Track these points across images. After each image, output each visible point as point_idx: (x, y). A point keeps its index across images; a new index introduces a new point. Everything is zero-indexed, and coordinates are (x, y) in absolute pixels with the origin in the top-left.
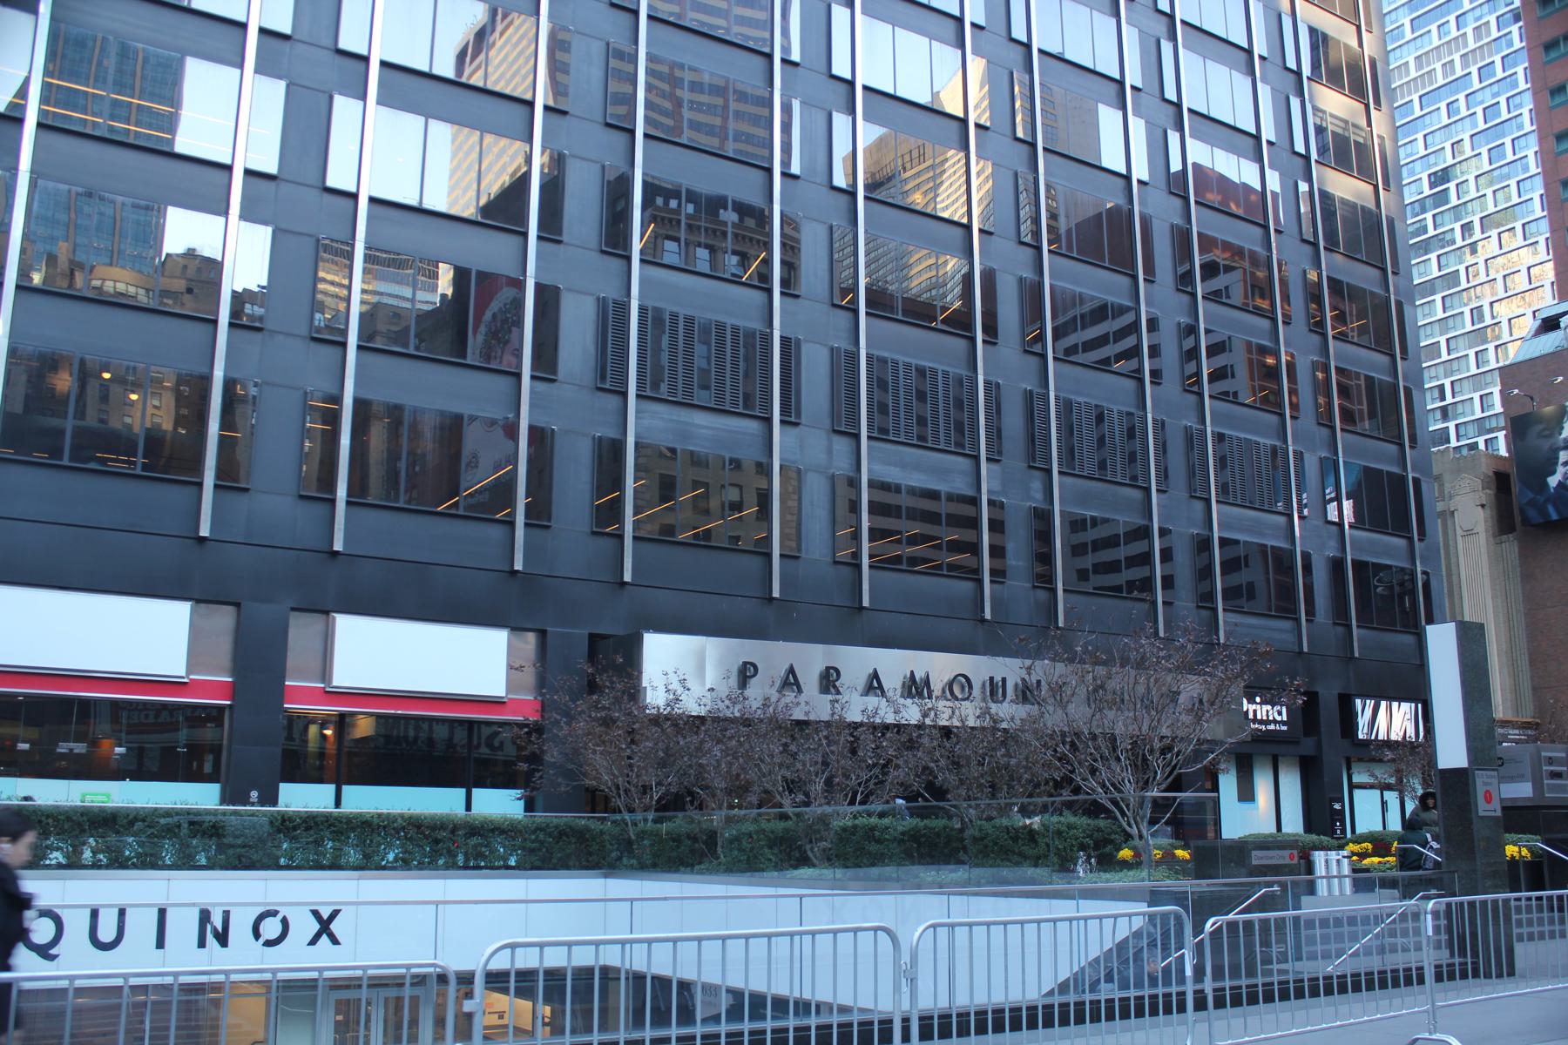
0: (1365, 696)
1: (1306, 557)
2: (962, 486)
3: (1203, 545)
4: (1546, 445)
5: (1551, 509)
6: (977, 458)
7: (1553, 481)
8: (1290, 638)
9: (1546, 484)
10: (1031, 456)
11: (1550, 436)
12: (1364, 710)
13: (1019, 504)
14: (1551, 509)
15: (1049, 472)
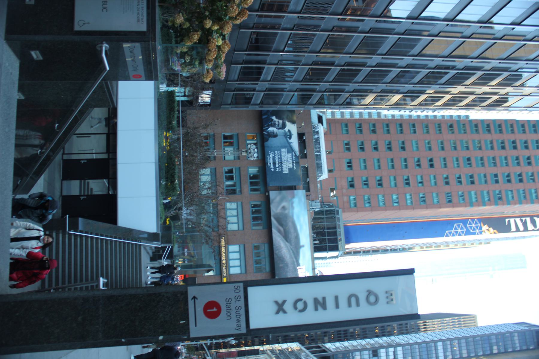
0: (213, 93)
1: (257, 84)
2: (291, 7)
3: (264, 63)
4: (285, 117)
5: (266, 116)
6: (300, 13)
7: (274, 118)
8: (232, 78)
9: (273, 116)
10: (298, 25)
11: (287, 118)
12: (210, 92)
13: (284, 23)
14: (266, 116)
15: (292, 29)
